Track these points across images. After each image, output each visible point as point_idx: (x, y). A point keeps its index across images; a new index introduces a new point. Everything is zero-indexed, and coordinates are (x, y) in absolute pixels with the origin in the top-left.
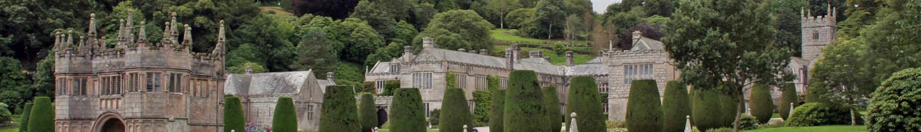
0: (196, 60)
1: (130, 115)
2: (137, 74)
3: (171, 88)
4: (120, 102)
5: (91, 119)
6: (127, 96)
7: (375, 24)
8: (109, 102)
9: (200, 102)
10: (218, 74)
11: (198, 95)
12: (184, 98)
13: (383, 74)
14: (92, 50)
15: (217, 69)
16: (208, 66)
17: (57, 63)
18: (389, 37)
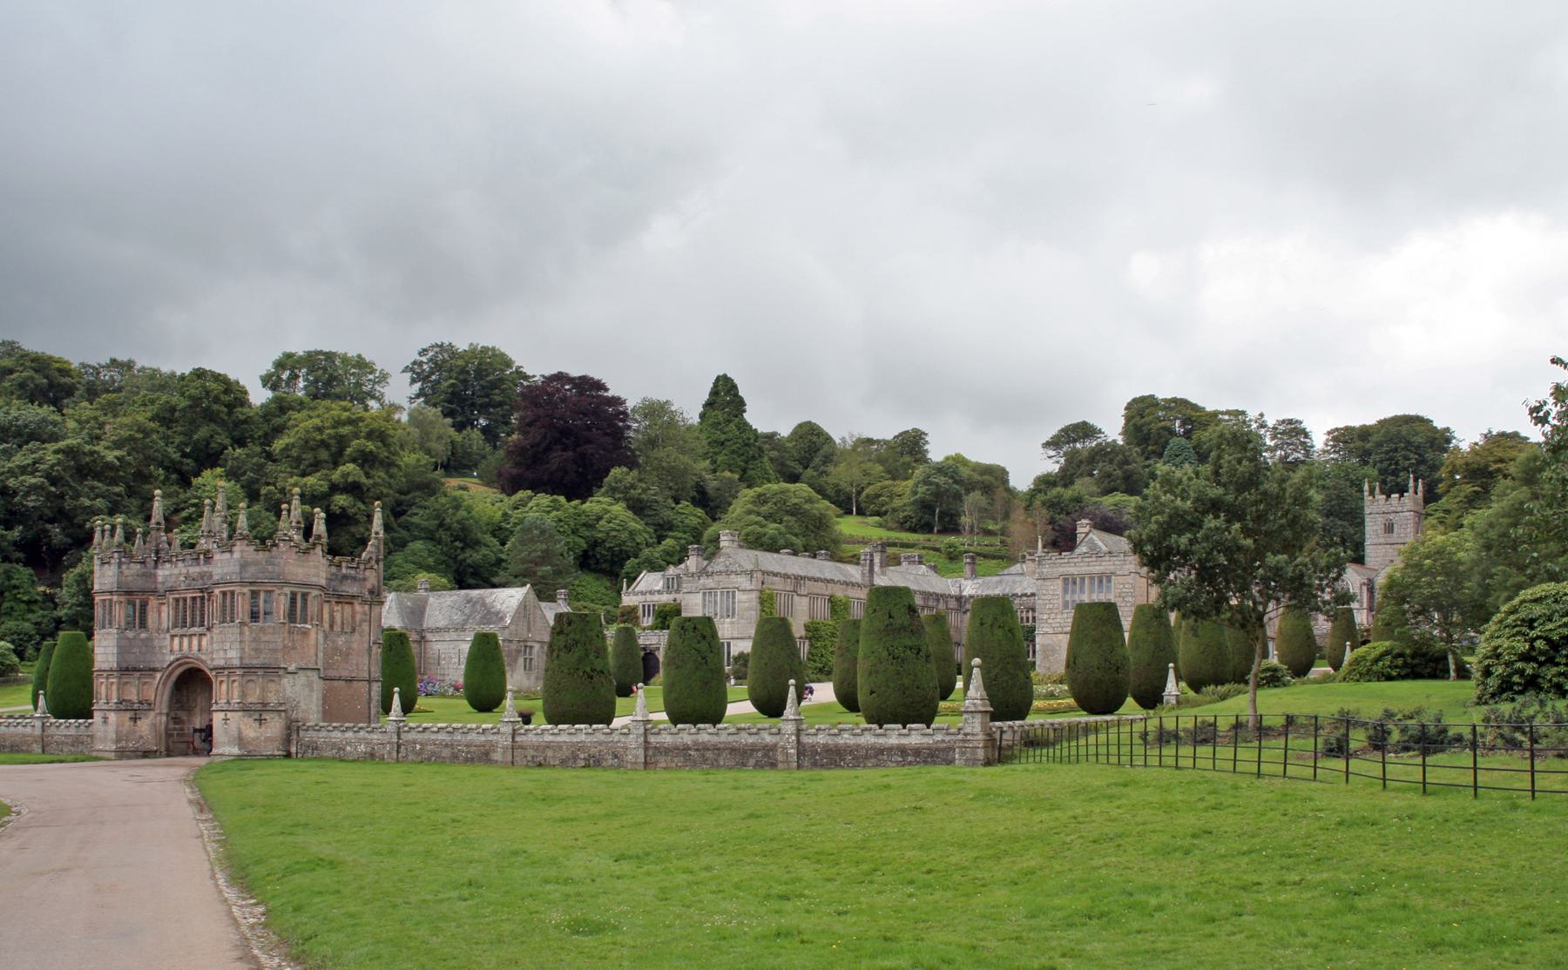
0: (334, 569)
1: (222, 663)
2: (233, 593)
3: (292, 616)
4: (205, 641)
5: (155, 670)
6: (216, 630)
7: (638, 507)
8: (186, 640)
9: (341, 641)
10: (371, 592)
11: (337, 628)
12: (313, 634)
13: (651, 593)
14: (157, 552)
15: (369, 585)
16: (354, 579)
17: (97, 575)
18: (662, 529)
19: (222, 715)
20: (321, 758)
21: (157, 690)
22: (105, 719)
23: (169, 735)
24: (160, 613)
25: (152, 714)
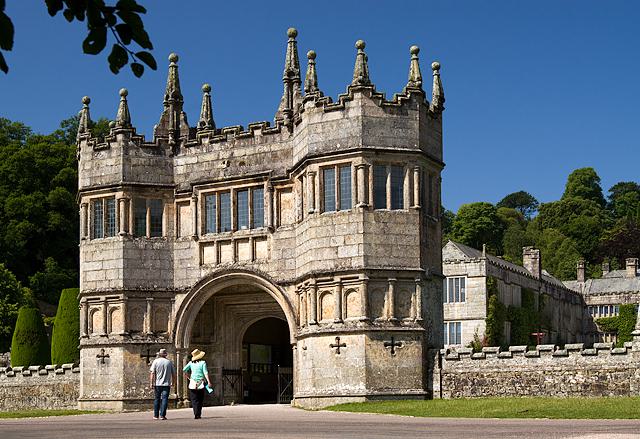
1: (330, 266)
4: (261, 246)
22: (103, 359)
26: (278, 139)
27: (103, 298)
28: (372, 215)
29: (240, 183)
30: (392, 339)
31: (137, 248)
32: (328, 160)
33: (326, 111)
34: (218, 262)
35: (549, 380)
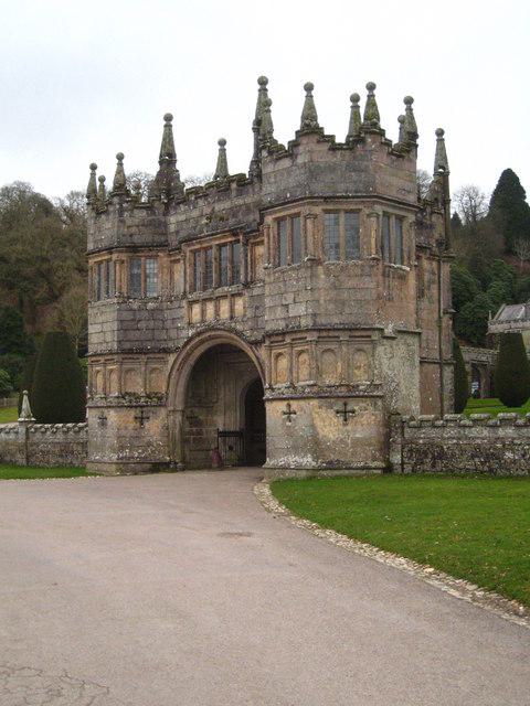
1: (281, 325)
4: (239, 304)
10: (440, 244)
15: (437, 236)
19: (282, 406)
20: (451, 473)
21: (167, 378)
23: (185, 441)
24: (171, 273)
25: (163, 412)
26: (251, 190)
27: (102, 359)
28: (320, 270)
29: (220, 238)
30: (345, 404)
31: (131, 310)
32: (280, 211)
33: (279, 159)
34: (203, 321)
35: (509, 455)
